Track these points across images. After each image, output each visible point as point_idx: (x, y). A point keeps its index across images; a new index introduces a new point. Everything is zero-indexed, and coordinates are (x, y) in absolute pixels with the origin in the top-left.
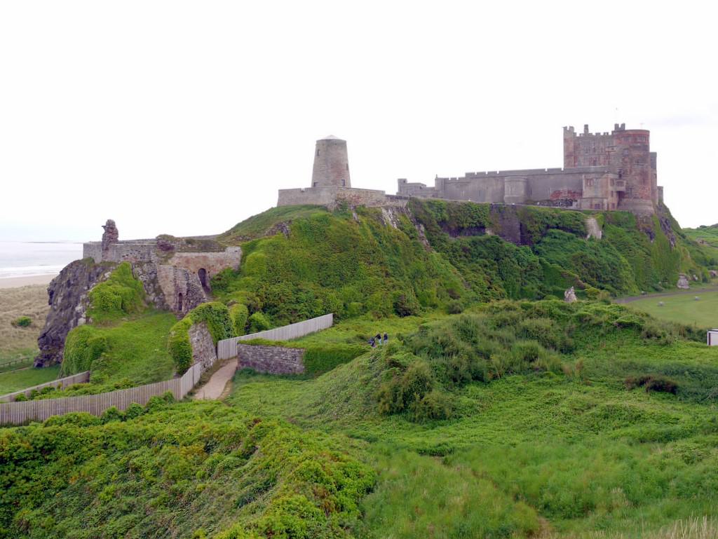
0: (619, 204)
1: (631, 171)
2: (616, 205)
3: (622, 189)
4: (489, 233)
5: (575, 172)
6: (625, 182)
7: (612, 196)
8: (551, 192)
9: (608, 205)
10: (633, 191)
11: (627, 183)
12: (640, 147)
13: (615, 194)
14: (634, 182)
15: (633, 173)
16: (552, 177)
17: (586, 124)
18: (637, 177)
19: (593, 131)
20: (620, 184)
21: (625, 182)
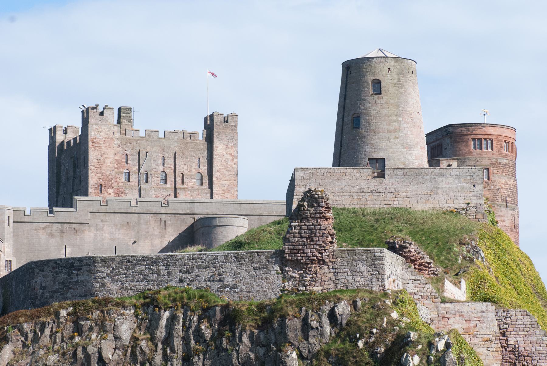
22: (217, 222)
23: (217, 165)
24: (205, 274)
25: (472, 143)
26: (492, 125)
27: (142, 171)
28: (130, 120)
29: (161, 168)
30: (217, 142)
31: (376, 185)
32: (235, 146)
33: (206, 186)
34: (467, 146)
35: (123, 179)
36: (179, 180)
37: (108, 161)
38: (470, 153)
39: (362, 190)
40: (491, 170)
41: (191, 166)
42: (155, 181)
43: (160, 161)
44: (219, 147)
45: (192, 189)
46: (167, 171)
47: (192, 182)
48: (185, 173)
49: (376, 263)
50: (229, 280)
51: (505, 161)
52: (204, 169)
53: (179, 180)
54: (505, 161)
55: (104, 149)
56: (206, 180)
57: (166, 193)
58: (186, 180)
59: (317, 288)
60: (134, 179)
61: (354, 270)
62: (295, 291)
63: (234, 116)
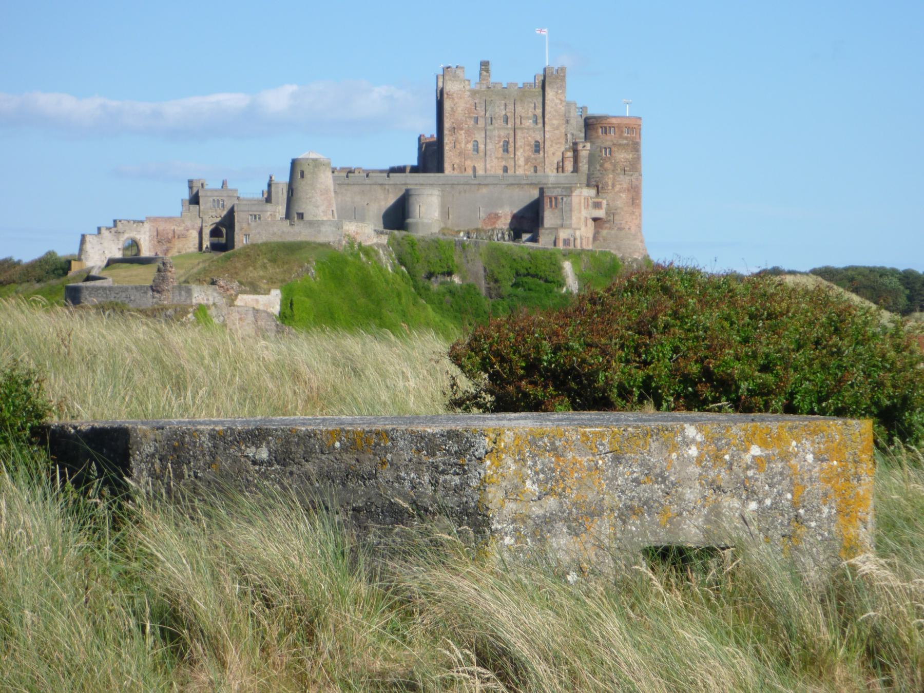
0: (595, 238)
1: (613, 186)
2: (591, 239)
3: (600, 213)
4: (456, 280)
5: (524, 182)
6: (604, 202)
7: (586, 225)
8: (483, 215)
9: (581, 239)
10: (616, 217)
11: (608, 204)
12: (627, 145)
13: (591, 222)
14: (619, 203)
15: (618, 187)
16: (484, 190)
17: (485, 59)
18: (623, 196)
19: (500, 76)
20: (597, 205)
21: (604, 202)
22: (412, 192)
23: (547, 108)
24: (124, 295)
25: (600, 130)
26: (615, 117)
27: (488, 115)
28: (487, 71)
29: (504, 113)
30: (547, 89)
31: (290, 229)
32: (563, 92)
33: (541, 125)
34: (597, 132)
35: (472, 122)
36: (518, 121)
37: (459, 110)
38: (598, 137)
39: (283, 232)
40: (613, 149)
41: (527, 110)
42: (499, 123)
43: (503, 107)
44: (550, 94)
45: (528, 129)
46: (509, 114)
47: (529, 123)
48: (523, 115)
49: (189, 292)
50: (132, 298)
51: (625, 142)
52: (539, 111)
53: (518, 121)
54: (625, 142)
55: (456, 100)
56: (540, 121)
57: (507, 132)
58: (523, 121)
59: (165, 302)
60: (481, 122)
61: (180, 295)
62: (157, 303)
63: (563, 69)
